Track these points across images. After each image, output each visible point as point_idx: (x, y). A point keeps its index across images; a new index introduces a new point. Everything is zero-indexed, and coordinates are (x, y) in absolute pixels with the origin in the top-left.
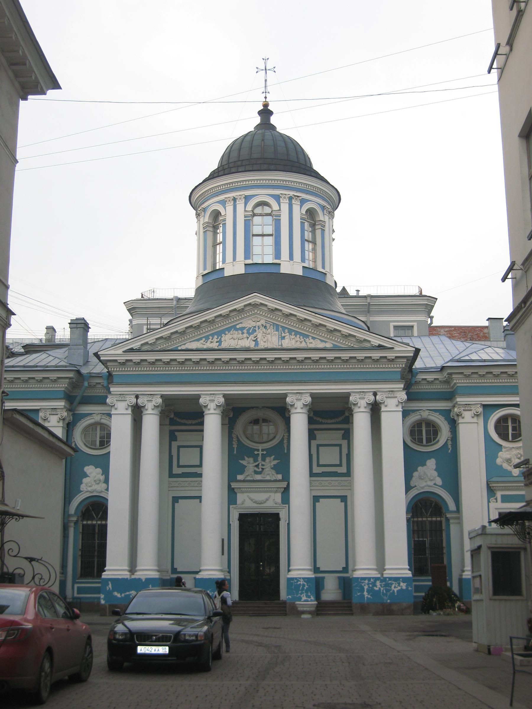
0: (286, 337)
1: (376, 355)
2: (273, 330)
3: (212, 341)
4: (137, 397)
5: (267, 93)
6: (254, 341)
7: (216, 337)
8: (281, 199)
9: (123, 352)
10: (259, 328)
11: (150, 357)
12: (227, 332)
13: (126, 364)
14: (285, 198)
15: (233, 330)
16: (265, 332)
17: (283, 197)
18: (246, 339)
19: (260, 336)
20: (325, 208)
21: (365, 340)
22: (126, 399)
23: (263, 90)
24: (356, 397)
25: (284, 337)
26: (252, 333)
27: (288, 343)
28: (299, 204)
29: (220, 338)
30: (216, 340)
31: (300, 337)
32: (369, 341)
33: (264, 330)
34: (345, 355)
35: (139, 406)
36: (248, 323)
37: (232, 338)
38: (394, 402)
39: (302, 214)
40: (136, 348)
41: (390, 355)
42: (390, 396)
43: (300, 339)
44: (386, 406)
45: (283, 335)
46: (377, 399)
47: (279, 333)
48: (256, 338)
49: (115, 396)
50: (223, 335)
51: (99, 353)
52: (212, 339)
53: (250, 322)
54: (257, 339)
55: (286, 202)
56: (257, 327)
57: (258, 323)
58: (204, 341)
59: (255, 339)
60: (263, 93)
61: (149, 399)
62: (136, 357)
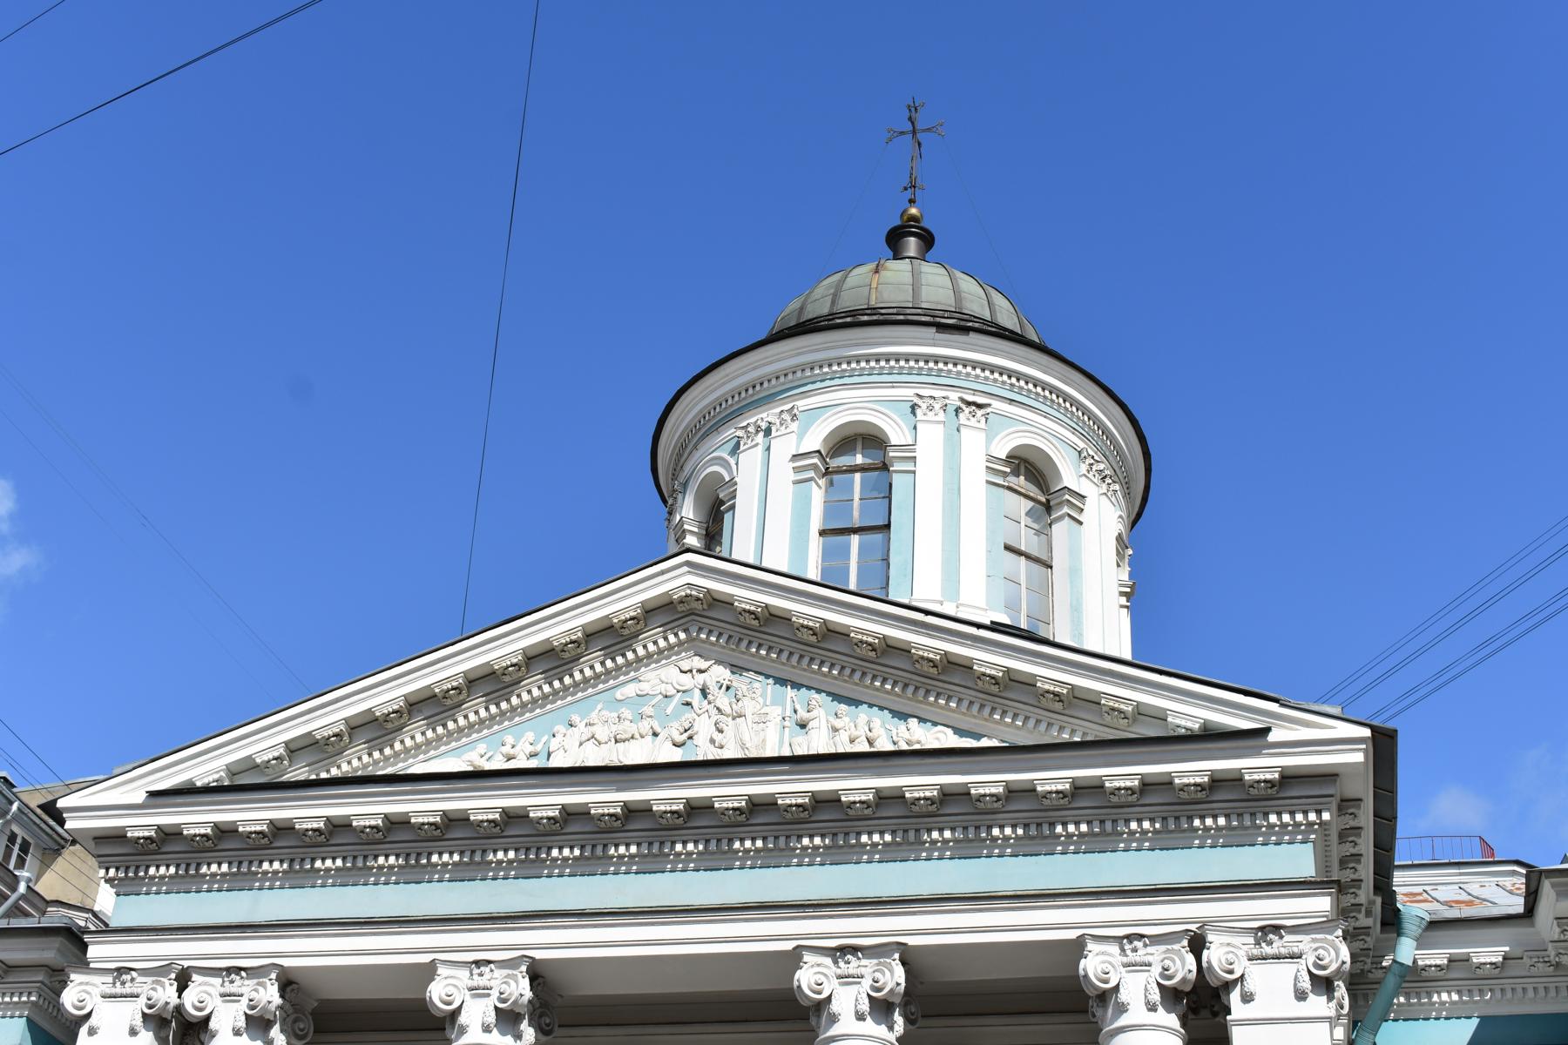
0: (810, 725)
1: (1191, 770)
2: (761, 700)
3: (512, 752)
4: (183, 981)
5: (916, 189)
6: (674, 745)
7: (530, 736)
8: (919, 412)
9: (153, 794)
10: (704, 692)
11: (252, 816)
12: (576, 718)
13: (164, 849)
14: (931, 408)
15: (599, 707)
16: (728, 711)
17: (924, 406)
18: (650, 738)
19: (704, 727)
20: (1083, 455)
21: (1141, 712)
22: (135, 991)
23: (906, 182)
24: (1110, 959)
25: (803, 726)
26: (676, 716)
27: (818, 742)
28: (982, 424)
29: (544, 739)
30: (530, 749)
31: (869, 723)
32: (1160, 716)
33: (723, 701)
34: (1053, 779)
35: (194, 1021)
36: (663, 678)
37: (593, 737)
38: (1285, 974)
39: (992, 458)
40: (206, 781)
41: (1258, 766)
42: (1267, 950)
43: (870, 731)
44: (1247, 998)
45: (802, 714)
46: (1204, 965)
47: (784, 710)
48: (689, 732)
49: (97, 979)
50: (560, 729)
51: (61, 804)
52: (513, 747)
53: (674, 671)
54: (690, 738)
55: (937, 418)
56: (697, 693)
57: (700, 678)
58: (482, 756)
59: (686, 735)
60: (906, 189)
61: (229, 988)
62: (196, 819)
